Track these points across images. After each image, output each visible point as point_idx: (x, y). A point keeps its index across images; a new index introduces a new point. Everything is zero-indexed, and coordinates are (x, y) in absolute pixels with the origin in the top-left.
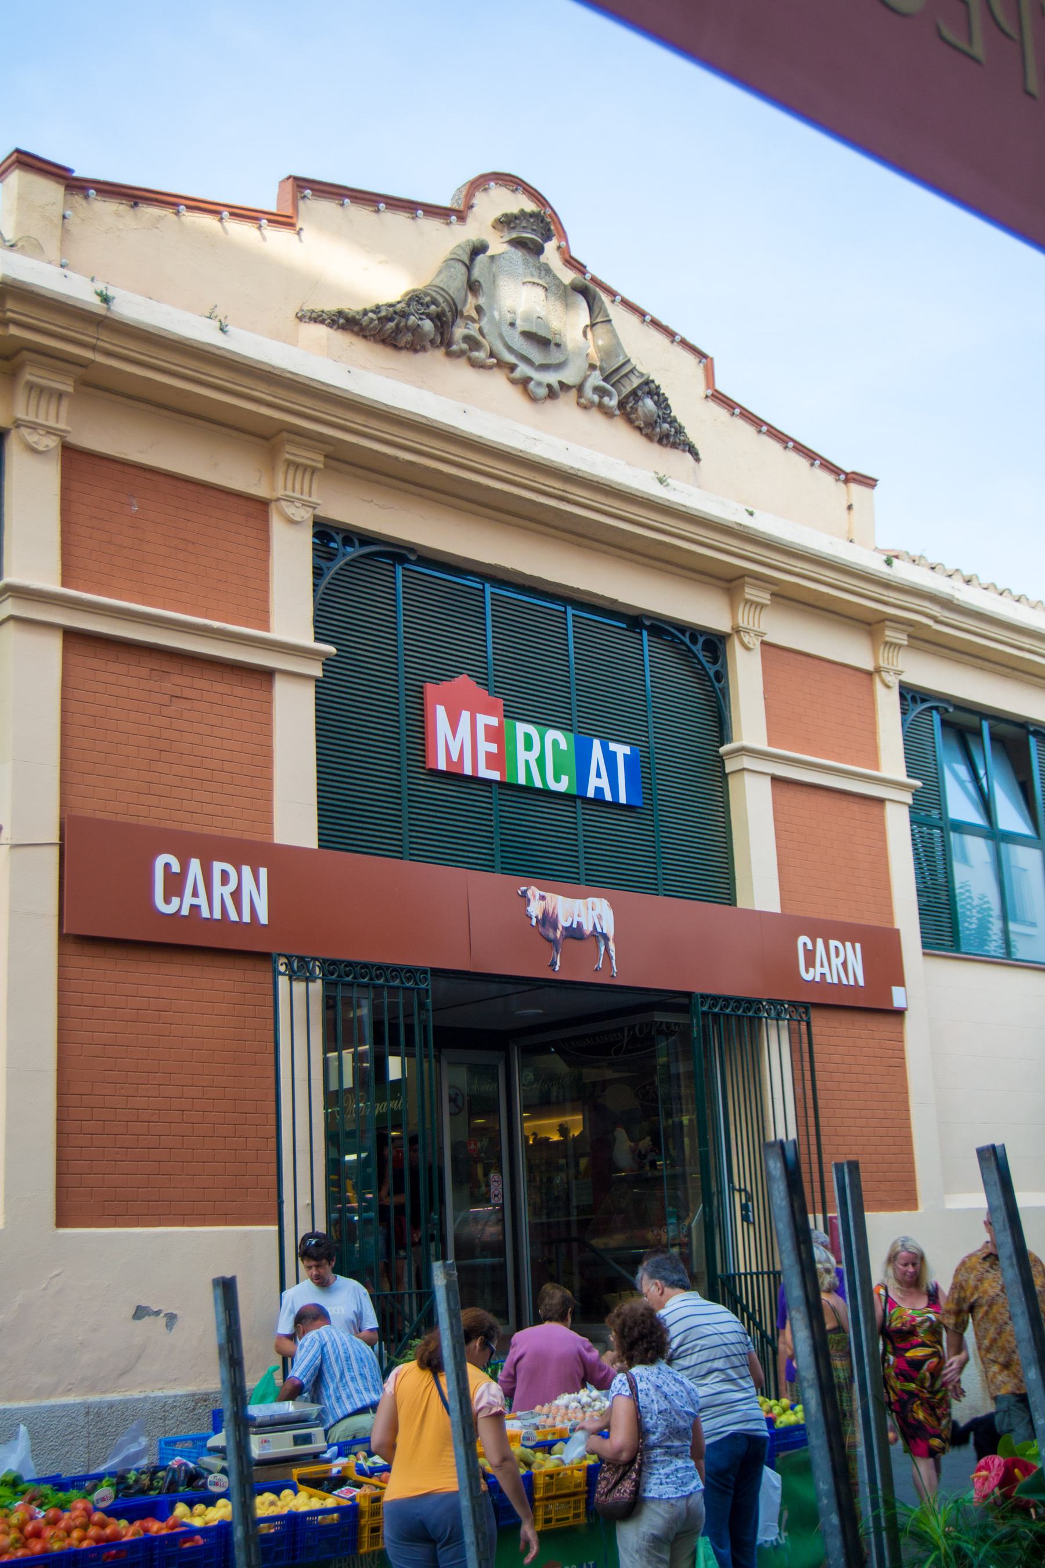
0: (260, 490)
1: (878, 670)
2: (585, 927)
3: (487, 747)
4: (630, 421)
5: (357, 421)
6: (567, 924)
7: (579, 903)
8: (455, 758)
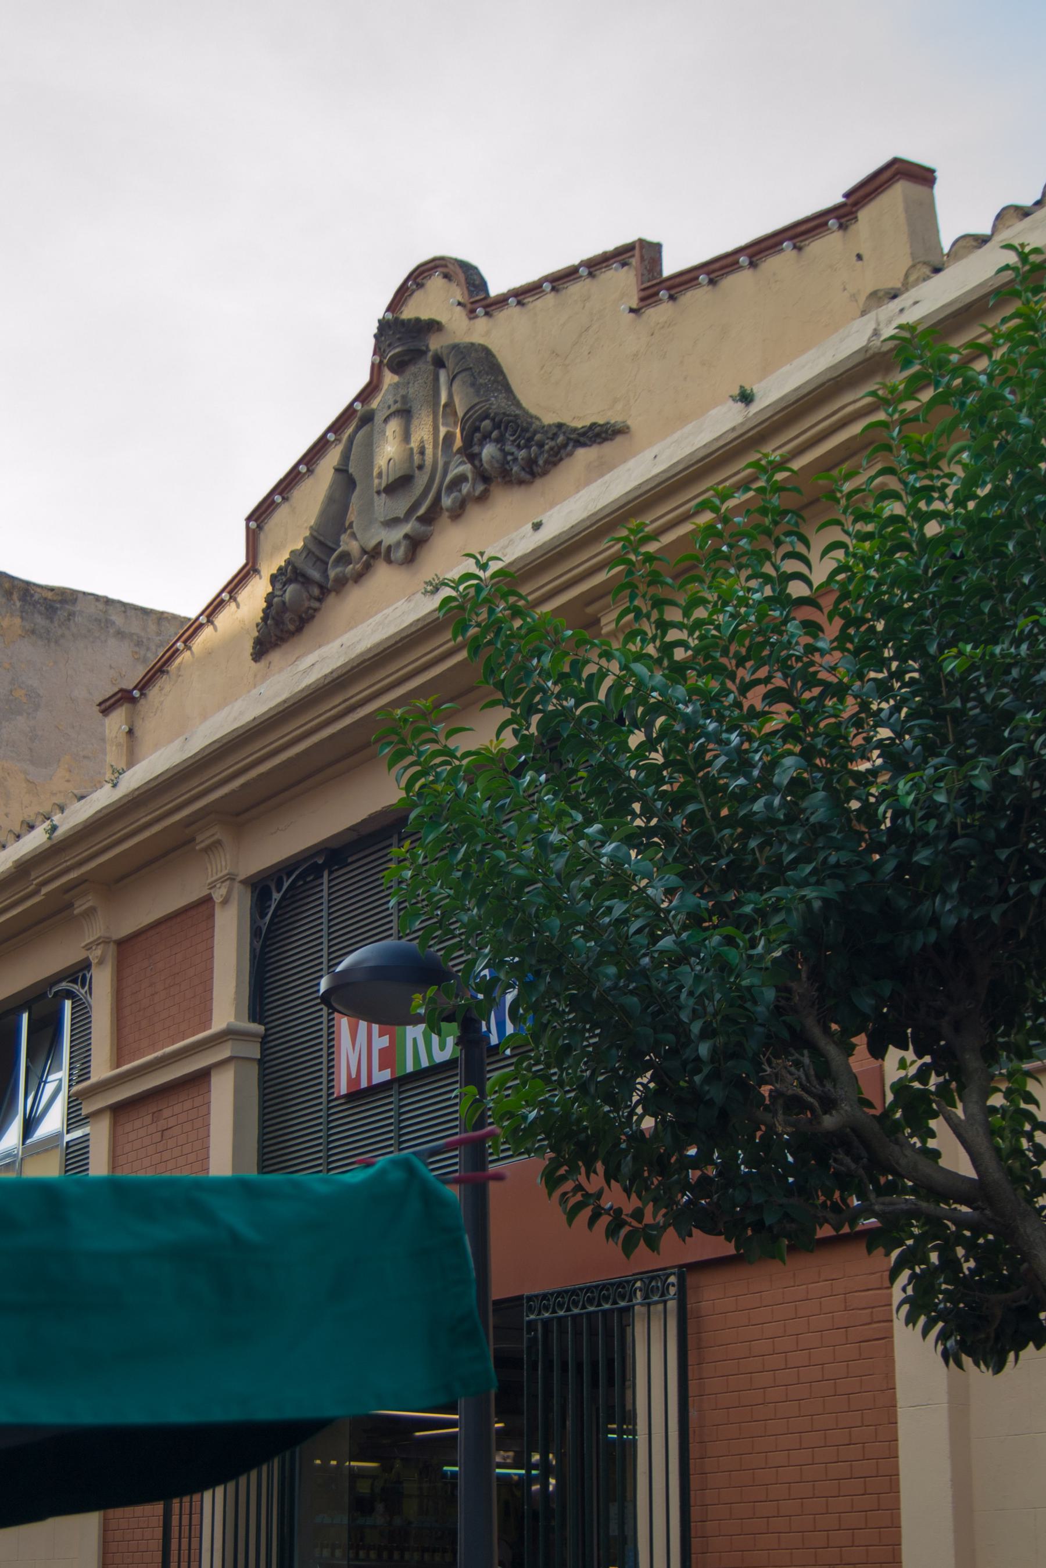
5: (195, 785)
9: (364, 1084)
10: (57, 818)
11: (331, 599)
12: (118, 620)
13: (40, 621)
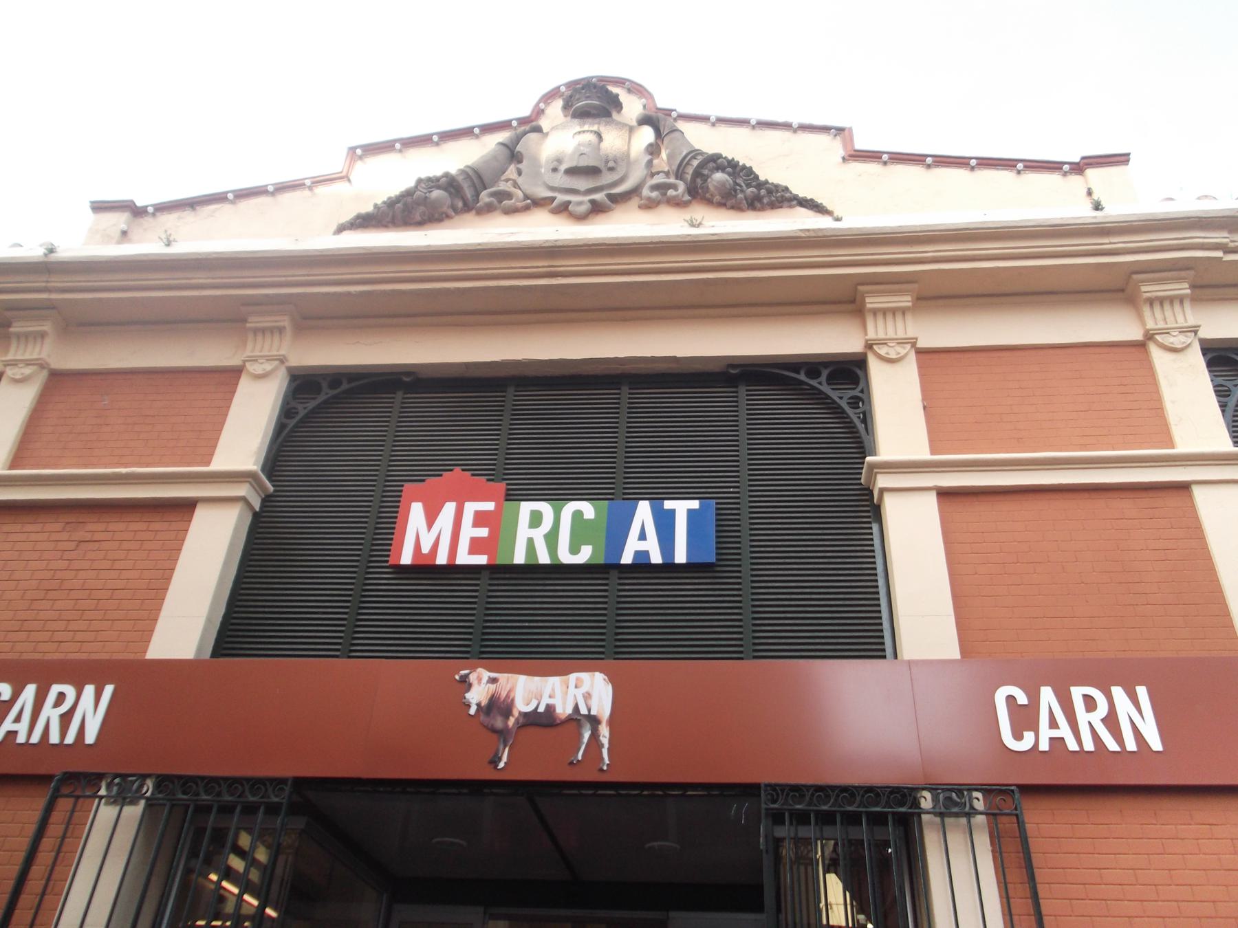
1: (1150, 336)
2: (559, 710)
3: (469, 531)
4: (709, 202)
7: (554, 681)
8: (426, 549)
9: (442, 559)
11: (470, 217)
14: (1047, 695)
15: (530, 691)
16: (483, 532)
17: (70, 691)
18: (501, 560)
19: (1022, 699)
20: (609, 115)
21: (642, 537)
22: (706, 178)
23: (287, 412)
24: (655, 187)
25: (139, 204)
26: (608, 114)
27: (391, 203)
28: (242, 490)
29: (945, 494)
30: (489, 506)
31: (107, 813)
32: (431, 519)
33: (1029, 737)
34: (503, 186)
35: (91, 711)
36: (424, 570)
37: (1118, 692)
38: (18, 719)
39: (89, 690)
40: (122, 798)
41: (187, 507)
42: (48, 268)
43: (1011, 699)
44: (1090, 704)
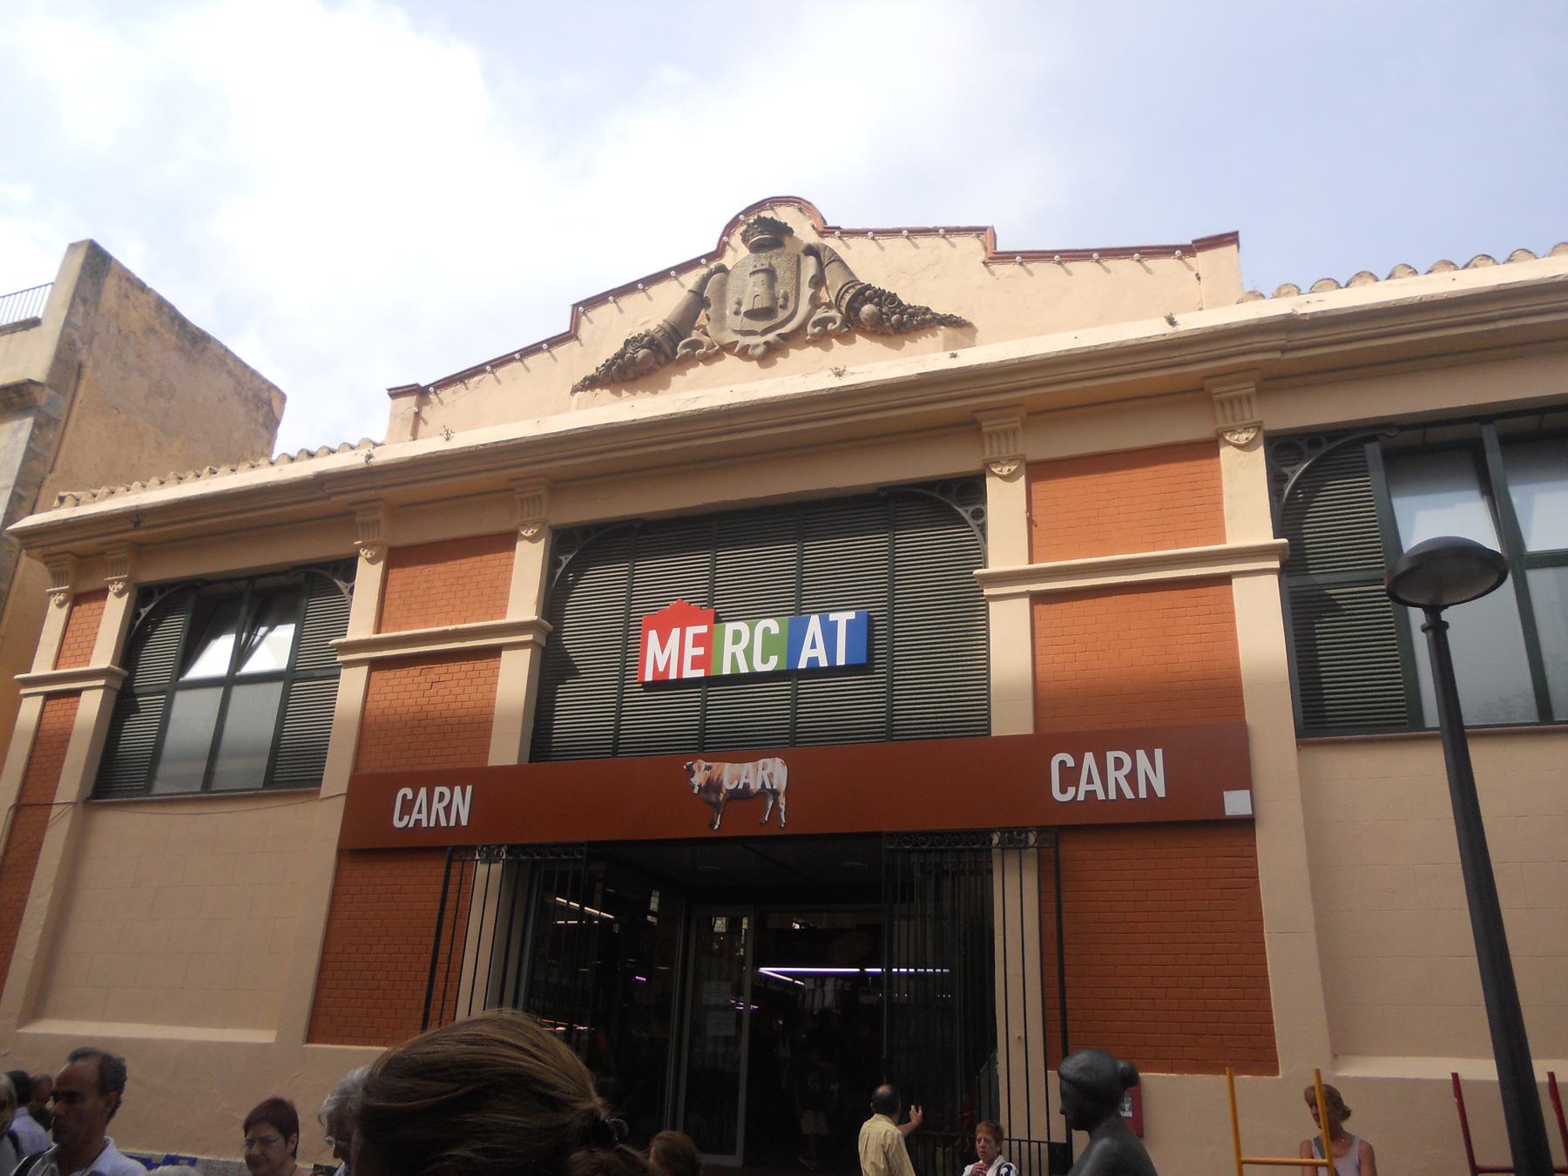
0: (508, 527)
3: (691, 651)
4: (864, 332)
6: (732, 787)
7: (749, 766)
8: (661, 669)
9: (673, 675)
10: (375, 452)
12: (231, 364)
13: (187, 345)
14: (1089, 759)
15: (735, 775)
16: (700, 651)
17: (446, 791)
18: (713, 673)
19: (1070, 762)
20: (780, 244)
21: (813, 646)
22: (857, 311)
23: (551, 563)
24: (815, 324)
25: (423, 384)
26: (780, 244)
27: (609, 365)
28: (529, 637)
29: (1037, 599)
30: (703, 629)
31: (482, 869)
32: (663, 643)
33: (1071, 790)
34: (695, 335)
35: (459, 804)
36: (661, 684)
37: (1141, 755)
38: (420, 812)
39: (458, 789)
40: (489, 860)
41: (494, 652)
42: (370, 475)
43: (1062, 763)
44: (1119, 764)
